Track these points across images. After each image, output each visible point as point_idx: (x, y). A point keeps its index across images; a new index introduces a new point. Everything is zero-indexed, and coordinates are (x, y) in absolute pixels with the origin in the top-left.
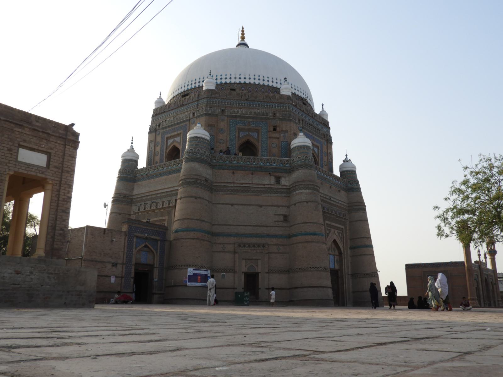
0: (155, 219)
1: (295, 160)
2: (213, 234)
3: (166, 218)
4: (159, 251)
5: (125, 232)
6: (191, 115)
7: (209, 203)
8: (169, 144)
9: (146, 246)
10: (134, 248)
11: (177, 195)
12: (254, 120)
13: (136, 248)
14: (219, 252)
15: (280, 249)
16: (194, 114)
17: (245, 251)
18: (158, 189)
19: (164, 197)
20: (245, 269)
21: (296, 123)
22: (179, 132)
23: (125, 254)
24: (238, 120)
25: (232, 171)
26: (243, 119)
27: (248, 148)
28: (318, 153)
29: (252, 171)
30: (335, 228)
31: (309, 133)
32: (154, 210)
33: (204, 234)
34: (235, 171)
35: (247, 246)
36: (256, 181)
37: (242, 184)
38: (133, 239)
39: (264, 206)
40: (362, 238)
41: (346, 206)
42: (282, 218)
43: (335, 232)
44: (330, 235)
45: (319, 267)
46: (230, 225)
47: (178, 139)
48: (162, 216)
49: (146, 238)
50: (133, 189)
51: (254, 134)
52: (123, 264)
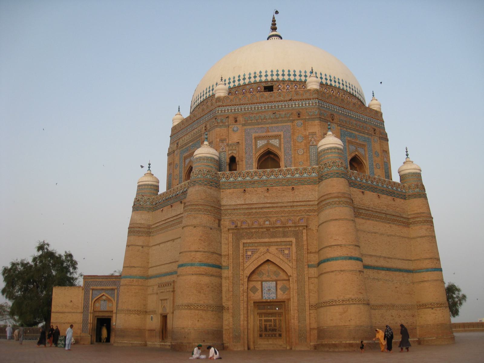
5: (82, 287)
7: (142, 247)
17: (161, 291)
20: (160, 311)
24: (184, 149)
28: (280, 144)
30: (269, 244)
31: (256, 126)
33: (132, 279)
35: (162, 286)
36: (174, 214)
37: (165, 220)
38: (89, 292)
41: (312, 205)
43: (268, 250)
44: (255, 256)
45: (180, 304)
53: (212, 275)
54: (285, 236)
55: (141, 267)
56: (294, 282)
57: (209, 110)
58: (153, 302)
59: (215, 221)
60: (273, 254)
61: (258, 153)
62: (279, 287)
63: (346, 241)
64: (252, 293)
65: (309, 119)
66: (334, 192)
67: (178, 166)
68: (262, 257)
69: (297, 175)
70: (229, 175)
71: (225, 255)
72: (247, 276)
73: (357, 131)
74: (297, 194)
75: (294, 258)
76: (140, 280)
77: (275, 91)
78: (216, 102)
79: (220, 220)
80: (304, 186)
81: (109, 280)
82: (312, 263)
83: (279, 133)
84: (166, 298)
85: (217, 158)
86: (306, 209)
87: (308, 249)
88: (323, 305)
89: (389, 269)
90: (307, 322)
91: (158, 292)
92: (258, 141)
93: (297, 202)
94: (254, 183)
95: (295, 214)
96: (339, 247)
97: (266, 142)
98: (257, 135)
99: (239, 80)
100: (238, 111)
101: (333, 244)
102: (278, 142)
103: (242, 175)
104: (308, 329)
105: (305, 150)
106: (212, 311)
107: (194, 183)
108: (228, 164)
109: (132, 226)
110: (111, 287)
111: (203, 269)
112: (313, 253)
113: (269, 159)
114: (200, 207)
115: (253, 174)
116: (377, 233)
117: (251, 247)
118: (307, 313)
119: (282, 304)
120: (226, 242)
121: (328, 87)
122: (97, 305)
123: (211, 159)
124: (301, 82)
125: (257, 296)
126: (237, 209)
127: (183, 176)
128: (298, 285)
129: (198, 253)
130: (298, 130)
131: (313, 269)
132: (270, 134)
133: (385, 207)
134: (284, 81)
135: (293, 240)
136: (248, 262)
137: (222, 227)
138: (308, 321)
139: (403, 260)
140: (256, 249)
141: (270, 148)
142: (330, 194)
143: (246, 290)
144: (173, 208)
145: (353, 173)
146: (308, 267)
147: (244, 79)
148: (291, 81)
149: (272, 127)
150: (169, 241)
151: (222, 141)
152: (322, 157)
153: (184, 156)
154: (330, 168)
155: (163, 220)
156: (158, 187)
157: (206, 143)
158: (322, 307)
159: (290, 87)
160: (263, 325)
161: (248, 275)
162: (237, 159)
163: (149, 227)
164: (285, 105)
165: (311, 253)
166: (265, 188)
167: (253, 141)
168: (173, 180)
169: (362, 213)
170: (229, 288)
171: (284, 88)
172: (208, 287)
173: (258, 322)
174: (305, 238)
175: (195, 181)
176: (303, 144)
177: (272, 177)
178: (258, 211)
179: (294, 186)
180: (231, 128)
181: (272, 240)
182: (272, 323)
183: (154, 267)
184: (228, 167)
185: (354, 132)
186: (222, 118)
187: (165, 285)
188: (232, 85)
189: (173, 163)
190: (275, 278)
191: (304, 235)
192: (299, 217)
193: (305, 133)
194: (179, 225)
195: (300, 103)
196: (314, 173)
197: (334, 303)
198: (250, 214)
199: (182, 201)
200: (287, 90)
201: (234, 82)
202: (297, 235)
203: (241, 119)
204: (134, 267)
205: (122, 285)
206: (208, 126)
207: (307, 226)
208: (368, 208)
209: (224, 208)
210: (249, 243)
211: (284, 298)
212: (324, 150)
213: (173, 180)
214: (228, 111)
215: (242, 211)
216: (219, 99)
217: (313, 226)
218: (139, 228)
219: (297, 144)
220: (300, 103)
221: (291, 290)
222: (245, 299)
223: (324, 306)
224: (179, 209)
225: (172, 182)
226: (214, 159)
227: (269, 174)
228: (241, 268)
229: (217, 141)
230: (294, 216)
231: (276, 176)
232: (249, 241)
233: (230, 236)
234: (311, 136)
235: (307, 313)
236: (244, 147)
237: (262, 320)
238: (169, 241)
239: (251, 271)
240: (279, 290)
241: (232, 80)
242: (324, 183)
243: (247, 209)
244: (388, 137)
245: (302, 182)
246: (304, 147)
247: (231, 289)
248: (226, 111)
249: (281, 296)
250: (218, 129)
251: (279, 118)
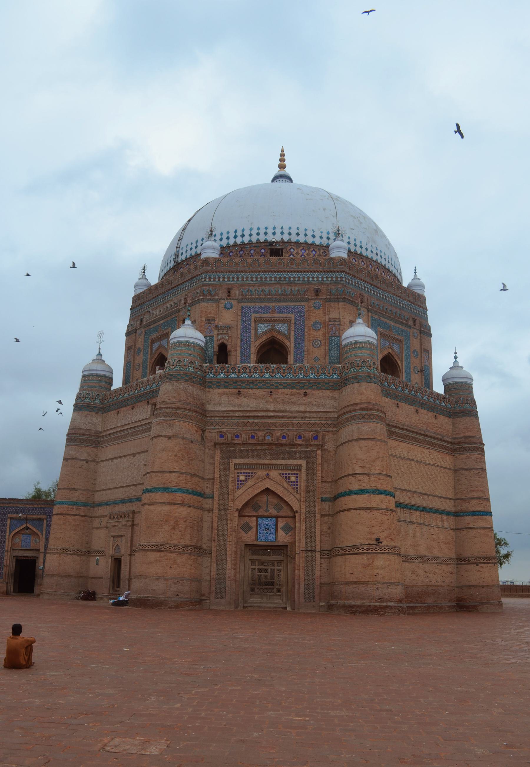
4: (44, 532)
7: (87, 462)
9: (27, 528)
12: (165, 320)
17: (113, 524)
21: (218, 301)
25: (117, 411)
26: (155, 325)
28: (289, 331)
31: (257, 304)
33: (70, 507)
34: (119, 410)
35: (116, 517)
36: (135, 419)
37: (124, 425)
38: (6, 521)
39: (137, 453)
40: (346, 476)
41: (330, 418)
43: (268, 474)
44: (250, 483)
51: (164, 342)
53: (190, 506)
54: (292, 457)
55: (84, 490)
56: (302, 520)
57: (190, 276)
58: (100, 539)
59: (197, 431)
60: (275, 481)
61: (258, 341)
62: (280, 525)
63: (375, 469)
64: (243, 532)
65: (330, 300)
66: (363, 402)
67: (141, 351)
68: (260, 484)
69: (312, 376)
70: (219, 370)
71: (209, 479)
72: (237, 510)
73: (392, 320)
74: (311, 402)
75: (302, 488)
76: (82, 507)
77: (285, 256)
78: (203, 266)
79: (204, 431)
80: (320, 391)
81: (36, 506)
82: (328, 496)
83: (289, 316)
84: (120, 534)
85: (203, 344)
86: (322, 422)
87: (322, 477)
88: (340, 553)
89: (424, 510)
90: (316, 575)
91: (109, 525)
92: (259, 325)
93: (310, 412)
94: (252, 383)
95: (307, 428)
96: (366, 477)
97: (270, 326)
98: (258, 315)
99: (235, 237)
100: (233, 280)
101: (358, 471)
102: (286, 328)
103: (237, 370)
104: (317, 583)
105: (323, 342)
106: (190, 554)
107: (170, 377)
108: (216, 353)
109: (73, 432)
110: (38, 517)
111: (179, 497)
112: (328, 482)
113: (273, 351)
114: (178, 411)
115: (252, 370)
116: (413, 460)
117: (245, 469)
118: (318, 562)
119: (282, 549)
120: (211, 461)
121: (357, 256)
122: (17, 540)
123: (196, 346)
124: (321, 246)
125: (250, 537)
126: (228, 417)
127: (148, 366)
128: (306, 524)
129: (174, 474)
130: (315, 313)
131: (328, 503)
132: (276, 316)
133: (424, 425)
134: (298, 243)
135: (303, 463)
136: (240, 490)
137: (206, 440)
138: (317, 574)
139: (443, 498)
140: (252, 473)
141: (275, 334)
142: (357, 404)
143: (236, 528)
144: (134, 410)
145: (386, 378)
146: (322, 501)
147: (243, 236)
148: (308, 244)
149: (280, 307)
150: (126, 456)
151: (209, 320)
152: (347, 353)
153: (150, 338)
154: (358, 368)
155: (120, 427)
156: (111, 379)
157: (188, 322)
158: (338, 555)
159: (307, 252)
160: (257, 576)
161: (239, 508)
162: (229, 347)
163: (98, 434)
164: (299, 278)
165: (326, 482)
166: (267, 390)
167: (253, 324)
168: (133, 370)
169: (395, 432)
170: (212, 523)
171: (297, 253)
172: (186, 521)
173: (250, 572)
174: (319, 461)
175: (172, 375)
176: (320, 333)
177: (278, 376)
178: (257, 421)
179: (307, 391)
180: (222, 303)
181: (275, 462)
182: (269, 574)
183: (103, 490)
184: (215, 357)
185: (388, 321)
186: (211, 289)
187: (119, 517)
188: (224, 243)
189: (133, 347)
190: (274, 513)
191: (319, 457)
192: (312, 433)
193: (324, 319)
194: (143, 435)
195: (320, 276)
196: (335, 374)
197: (356, 552)
198: (245, 424)
199: (149, 401)
200: (301, 256)
201: (228, 238)
202: (309, 457)
203: (237, 292)
205: (55, 515)
207: (322, 446)
208: (403, 425)
209: (211, 414)
210: (243, 464)
211: (286, 541)
212: (351, 344)
213: (133, 370)
214: (219, 280)
215: (236, 420)
216: (206, 262)
217: (330, 446)
218: (84, 435)
219: (313, 333)
220: (320, 276)
221: (297, 531)
222: (235, 540)
223: (342, 555)
224: (143, 412)
225: (131, 374)
226: (199, 346)
227: (272, 372)
228: (230, 497)
229: (201, 320)
230: (305, 430)
231: (283, 374)
232: (242, 461)
233: (216, 453)
234: (332, 323)
235: (318, 562)
236: (239, 332)
237: (254, 569)
238: (126, 456)
239: (244, 502)
240: (279, 530)
241: (225, 236)
242: (348, 390)
243: (241, 417)
244: (432, 332)
245: (317, 385)
246: (322, 337)
247: (215, 526)
248: (217, 280)
249: (282, 538)
250: (204, 304)
251: (289, 295)
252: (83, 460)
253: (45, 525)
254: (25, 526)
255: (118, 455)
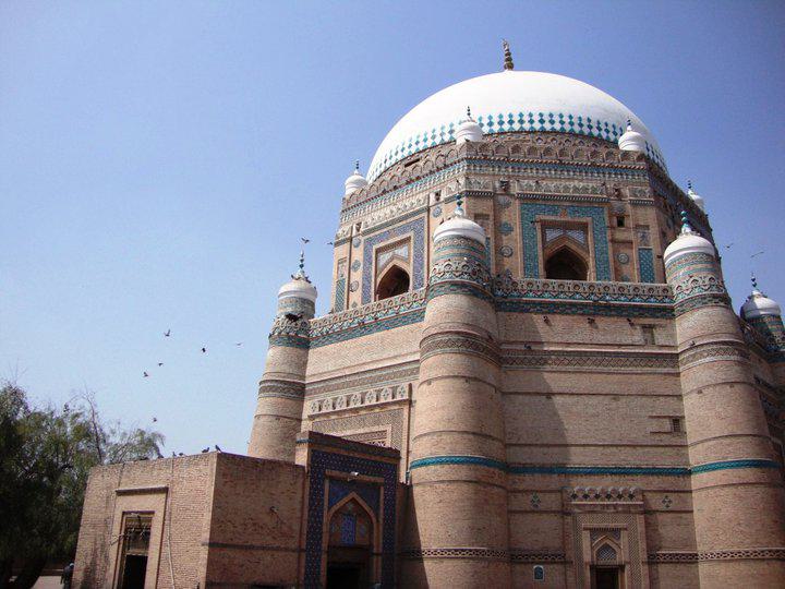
0: (361, 431)
1: (684, 288)
2: (509, 468)
3: (389, 429)
4: (382, 511)
6: (432, 197)
8: (381, 263)
10: (326, 507)
11: (418, 372)
13: (329, 509)
14: (526, 512)
15: (670, 502)
16: (438, 195)
18: (364, 361)
19: (380, 379)
22: (404, 236)
23: (305, 523)
27: (564, 264)
29: (590, 314)
32: (356, 410)
33: (492, 470)
34: (550, 317)
35: (592, 495)
38: (323, 485)
42: (667, 425)
46: (548, 446)
47: (402, 251)
48: (377, 423)
49: (354, 482)
50: (305, 363)
51: (577, 235)
52: (300, 550)
67: (511, 230)
84: (612, 525)
204: (490, 436)
206: (626, 192)
252: (494, 386)
253: (382, 497)
254: (350, 496)
255: (567, 391)
